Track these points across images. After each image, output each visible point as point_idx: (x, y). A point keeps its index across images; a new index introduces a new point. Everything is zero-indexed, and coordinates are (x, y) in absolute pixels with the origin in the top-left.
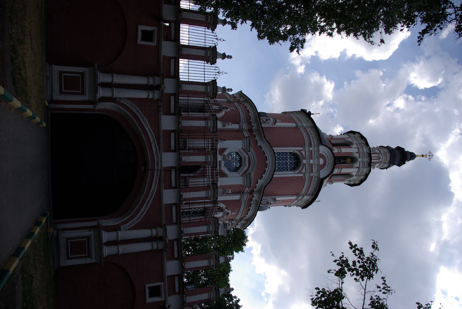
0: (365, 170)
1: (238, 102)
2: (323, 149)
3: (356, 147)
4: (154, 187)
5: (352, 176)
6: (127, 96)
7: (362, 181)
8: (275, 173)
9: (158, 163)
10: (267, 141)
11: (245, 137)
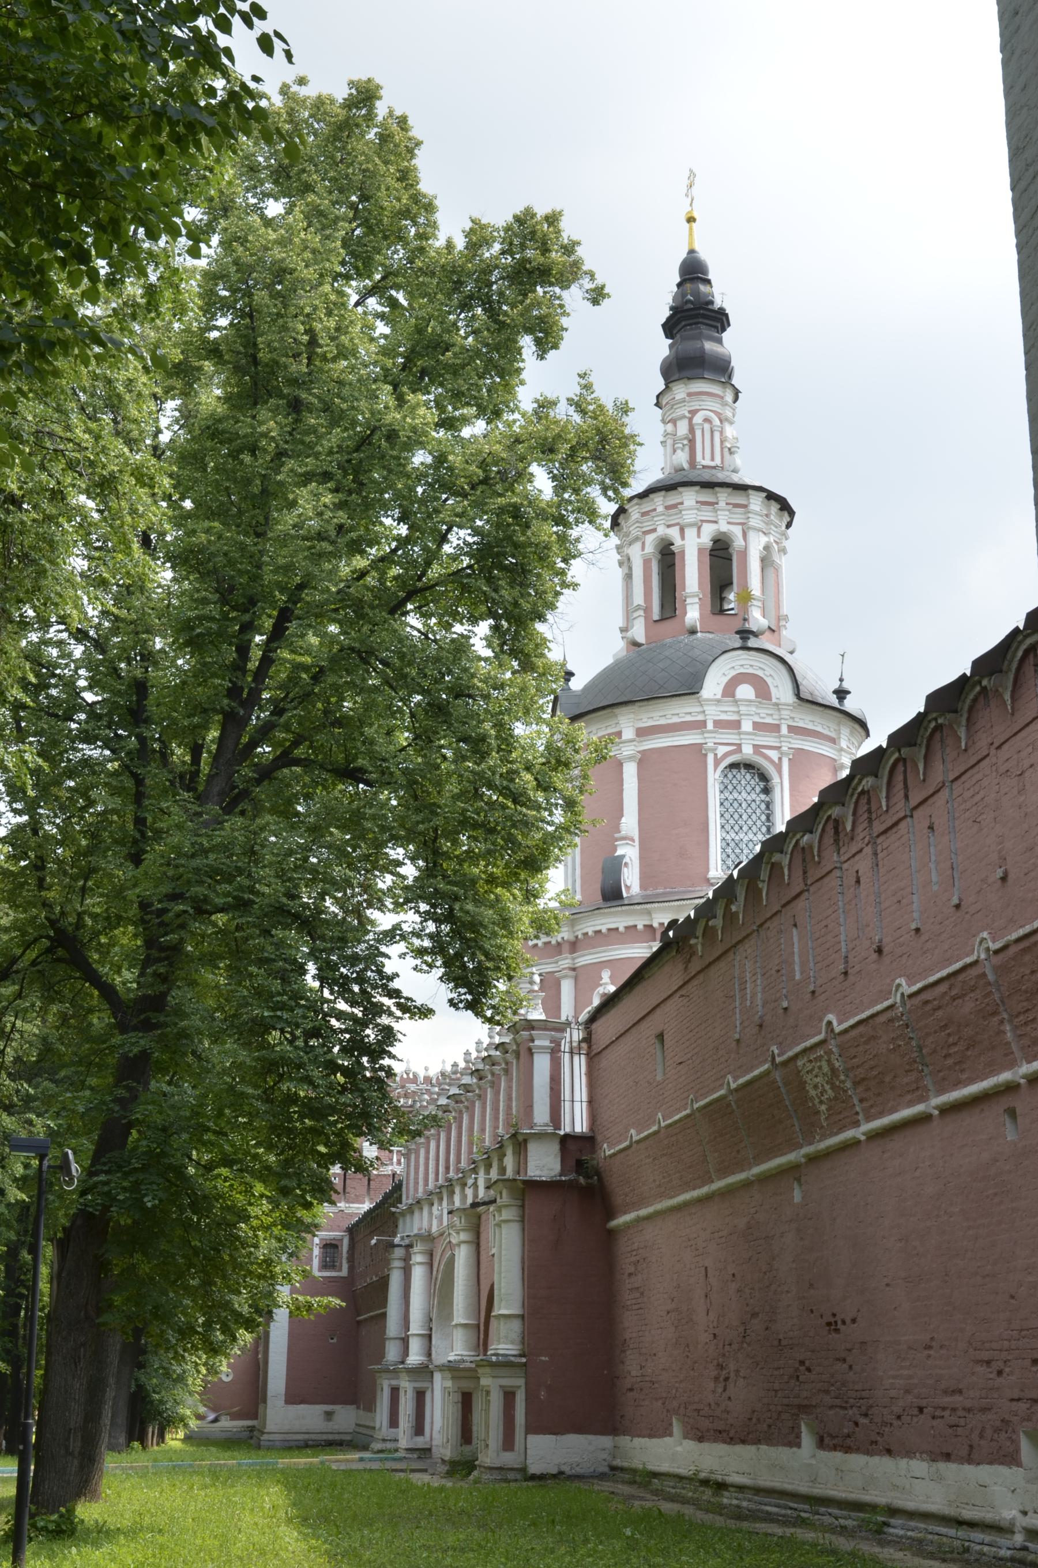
0: (756, 502)
2: (713, 685)
5: (767, 548)
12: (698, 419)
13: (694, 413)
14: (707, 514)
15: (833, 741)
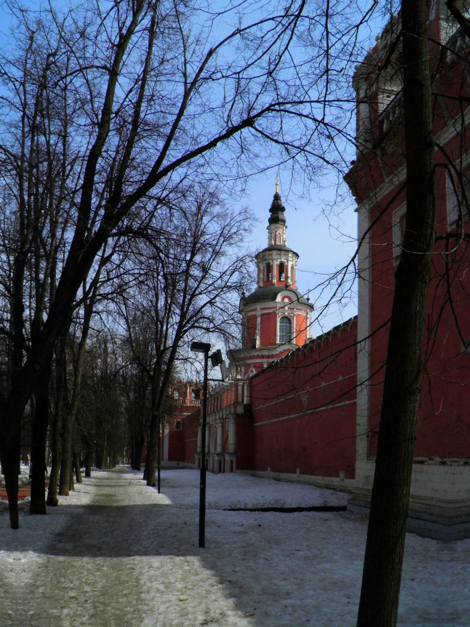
2: (279, 298)
5: (293, 265)
12: (277, 233)
13: (276, 232)
14: (278, 257)
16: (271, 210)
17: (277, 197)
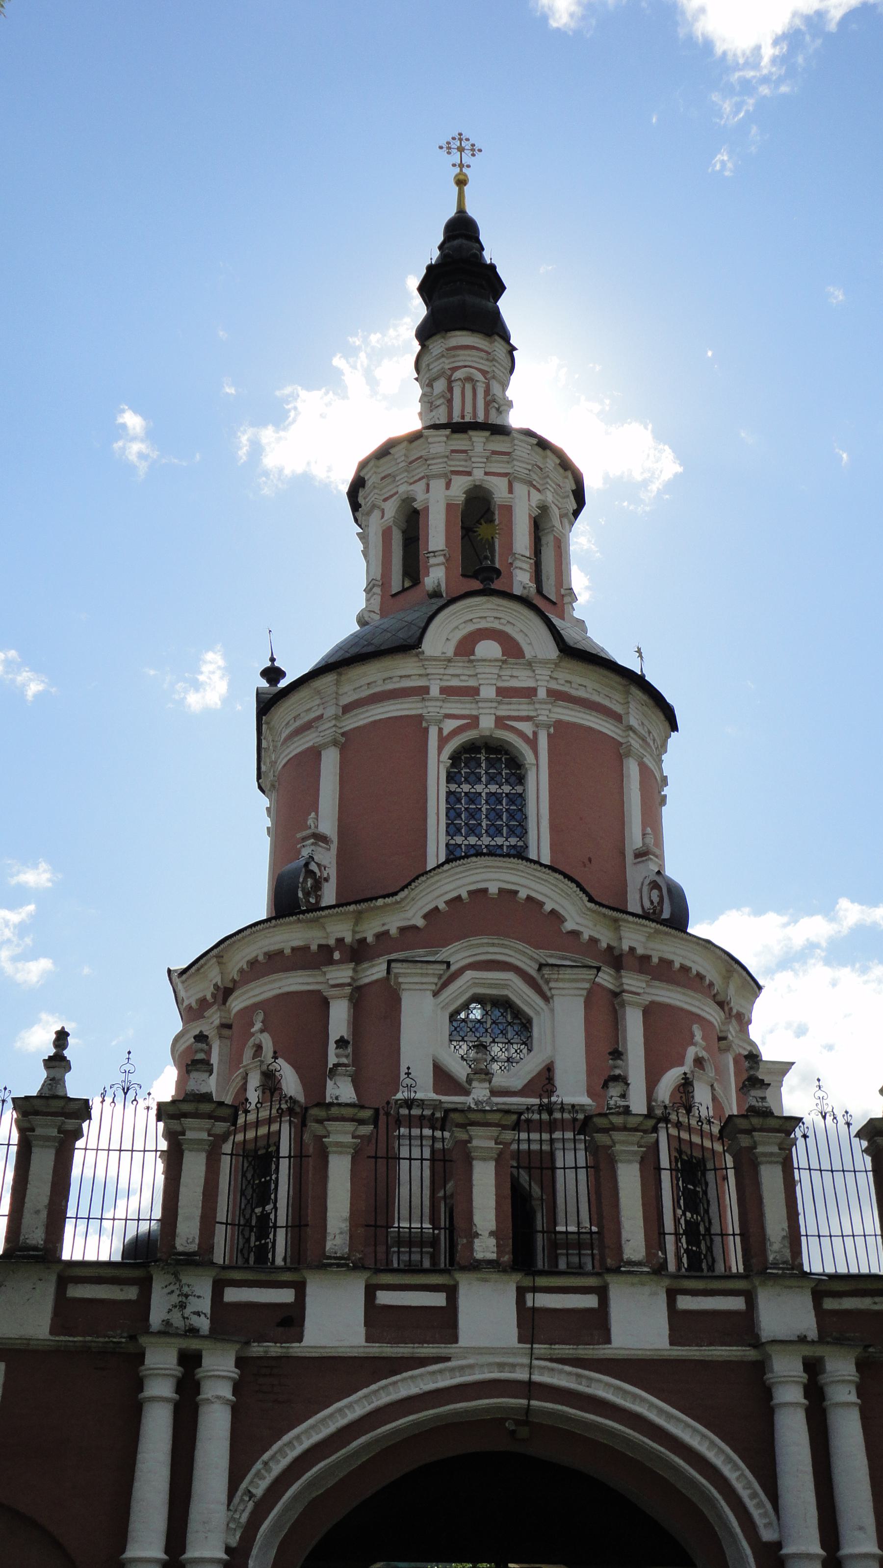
1: (225, 993)
2: (440, 639)
3: (423, 483)
4: (605, 1387)
5: (544, 509)
6: (221, 1494)
7: (565, 464)
8: (533, 855)
9: (501, 1366)
10: (406, 886)
11: (387, 979)
12: (458, 374)
14: (458, 464)
15: (618, 718)
16: (425, 289)
17: (461, 231)
